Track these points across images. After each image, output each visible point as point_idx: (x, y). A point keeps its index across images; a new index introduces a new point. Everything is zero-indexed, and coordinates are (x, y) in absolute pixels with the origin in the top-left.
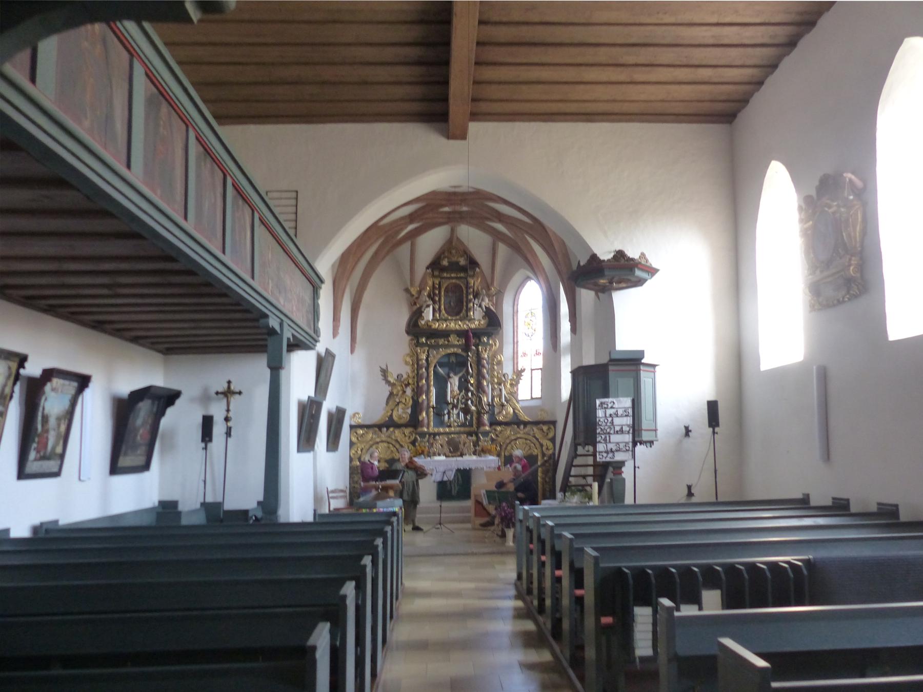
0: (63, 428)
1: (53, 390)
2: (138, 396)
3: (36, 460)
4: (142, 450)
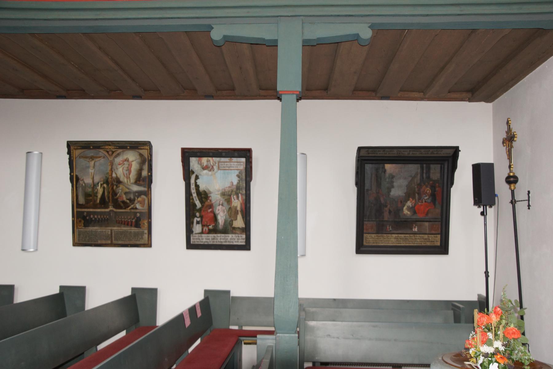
0: (237, 203)
3: (202, 233)
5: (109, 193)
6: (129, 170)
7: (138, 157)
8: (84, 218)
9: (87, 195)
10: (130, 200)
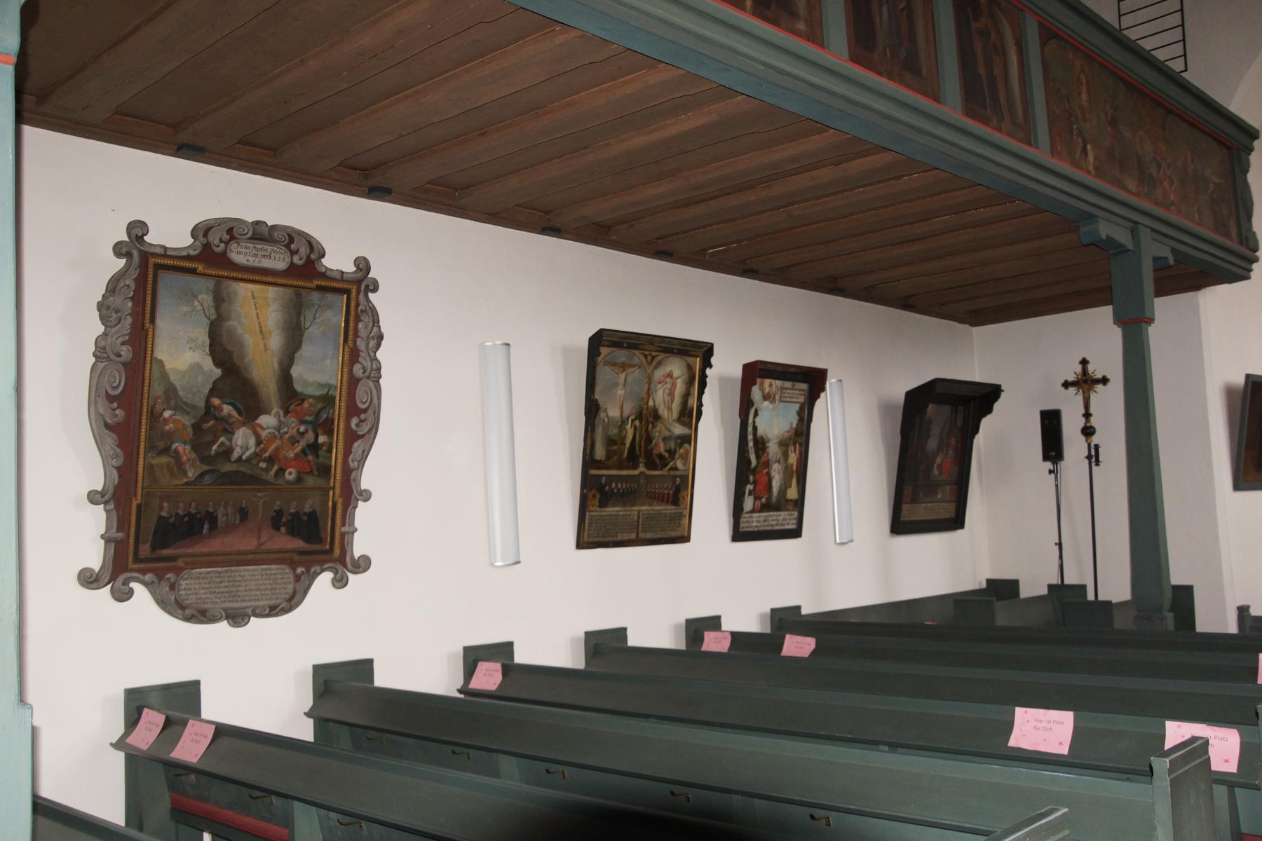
0: (793, 459)
1: (766, 397)
2: (918, 399)
3: (753, 511)
4: (946, 492)
5: (641, 437)
6: (672, 394)
7: (685, 370)
8: (601, 489)
9: (610, 442)
10: (669, 451)
